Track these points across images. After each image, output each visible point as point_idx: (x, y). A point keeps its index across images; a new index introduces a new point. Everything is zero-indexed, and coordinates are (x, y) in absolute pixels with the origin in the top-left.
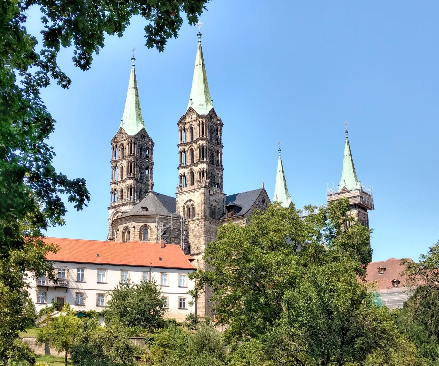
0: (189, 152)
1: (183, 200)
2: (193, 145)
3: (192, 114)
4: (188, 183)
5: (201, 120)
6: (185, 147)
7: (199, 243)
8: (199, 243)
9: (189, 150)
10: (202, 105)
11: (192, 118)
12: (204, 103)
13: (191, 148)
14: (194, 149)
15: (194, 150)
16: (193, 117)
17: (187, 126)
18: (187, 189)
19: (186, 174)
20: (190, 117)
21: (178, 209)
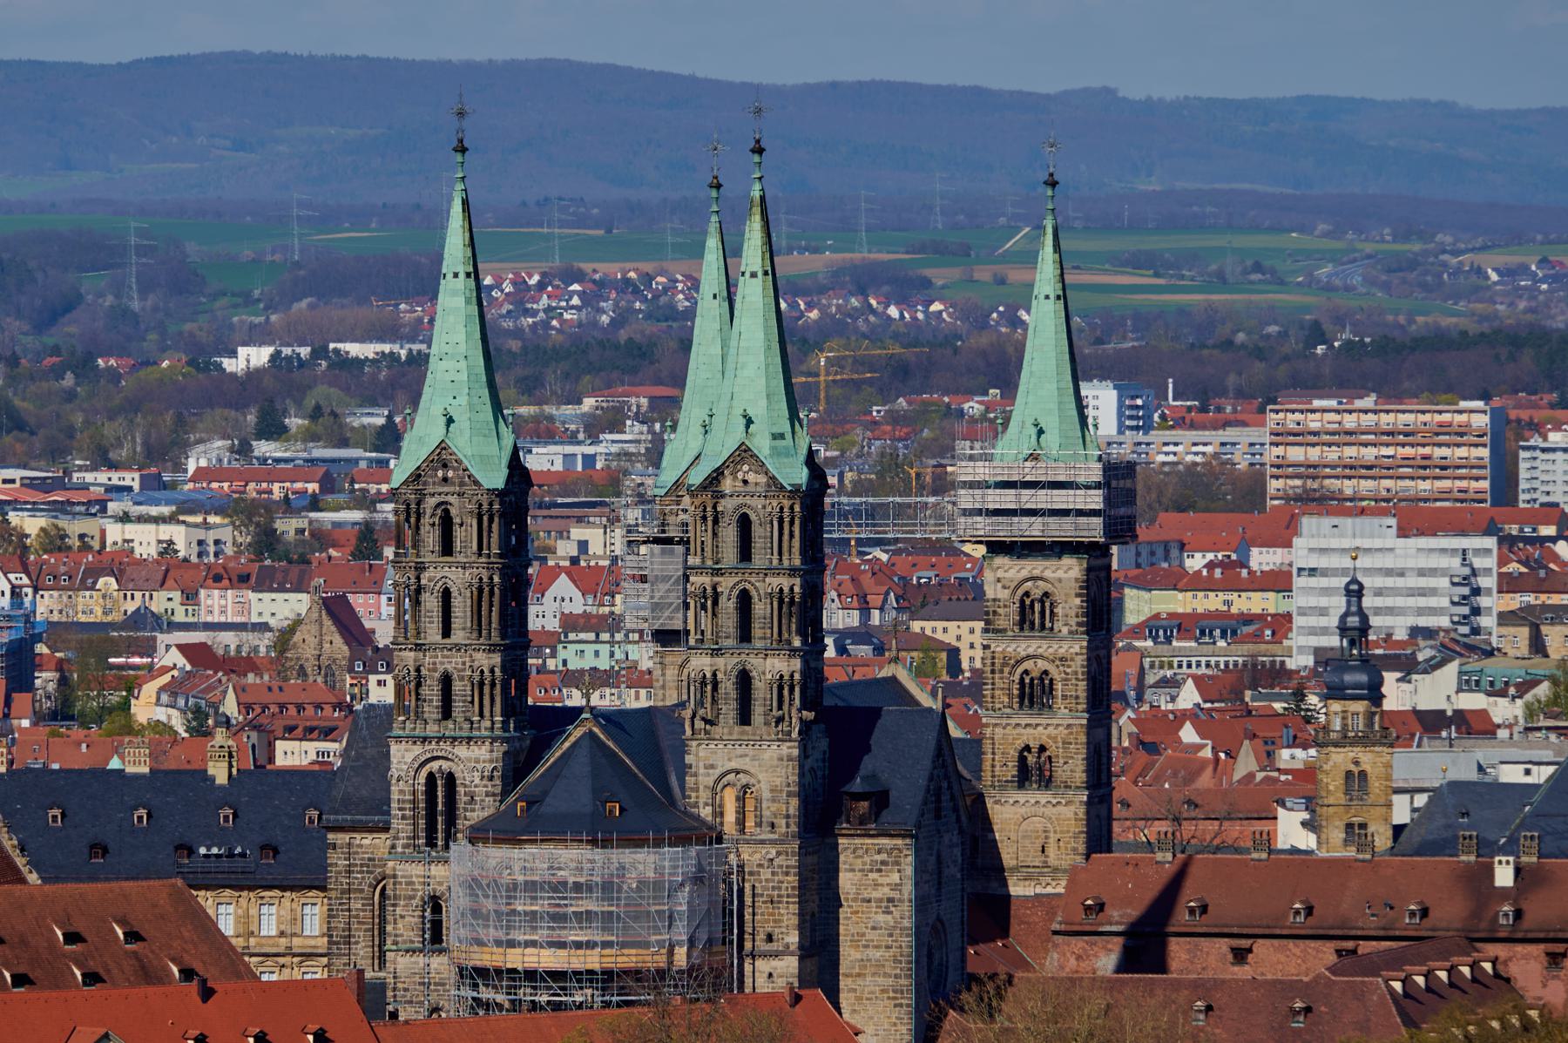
0: (734, 600)
1: (712, 767)
2: (753, 580)
3: (746, 468)
4: (729, 709)
5: (786, 503)
6: (716, 579)
7: (775, 921)
8: (775, 921)
9: (736, 592)
10: (782, 436)
11: (745, 482)
12: (787, 428)
13: (741, 586)
14: (754, 593)
15: (755, 599)
16: (751, 477)
17: (726, 505)
18: (730, 734)
19: (720, 676)
20: (740, 475)
21: (693, 795)
